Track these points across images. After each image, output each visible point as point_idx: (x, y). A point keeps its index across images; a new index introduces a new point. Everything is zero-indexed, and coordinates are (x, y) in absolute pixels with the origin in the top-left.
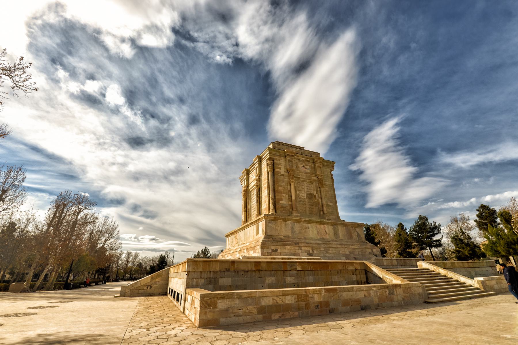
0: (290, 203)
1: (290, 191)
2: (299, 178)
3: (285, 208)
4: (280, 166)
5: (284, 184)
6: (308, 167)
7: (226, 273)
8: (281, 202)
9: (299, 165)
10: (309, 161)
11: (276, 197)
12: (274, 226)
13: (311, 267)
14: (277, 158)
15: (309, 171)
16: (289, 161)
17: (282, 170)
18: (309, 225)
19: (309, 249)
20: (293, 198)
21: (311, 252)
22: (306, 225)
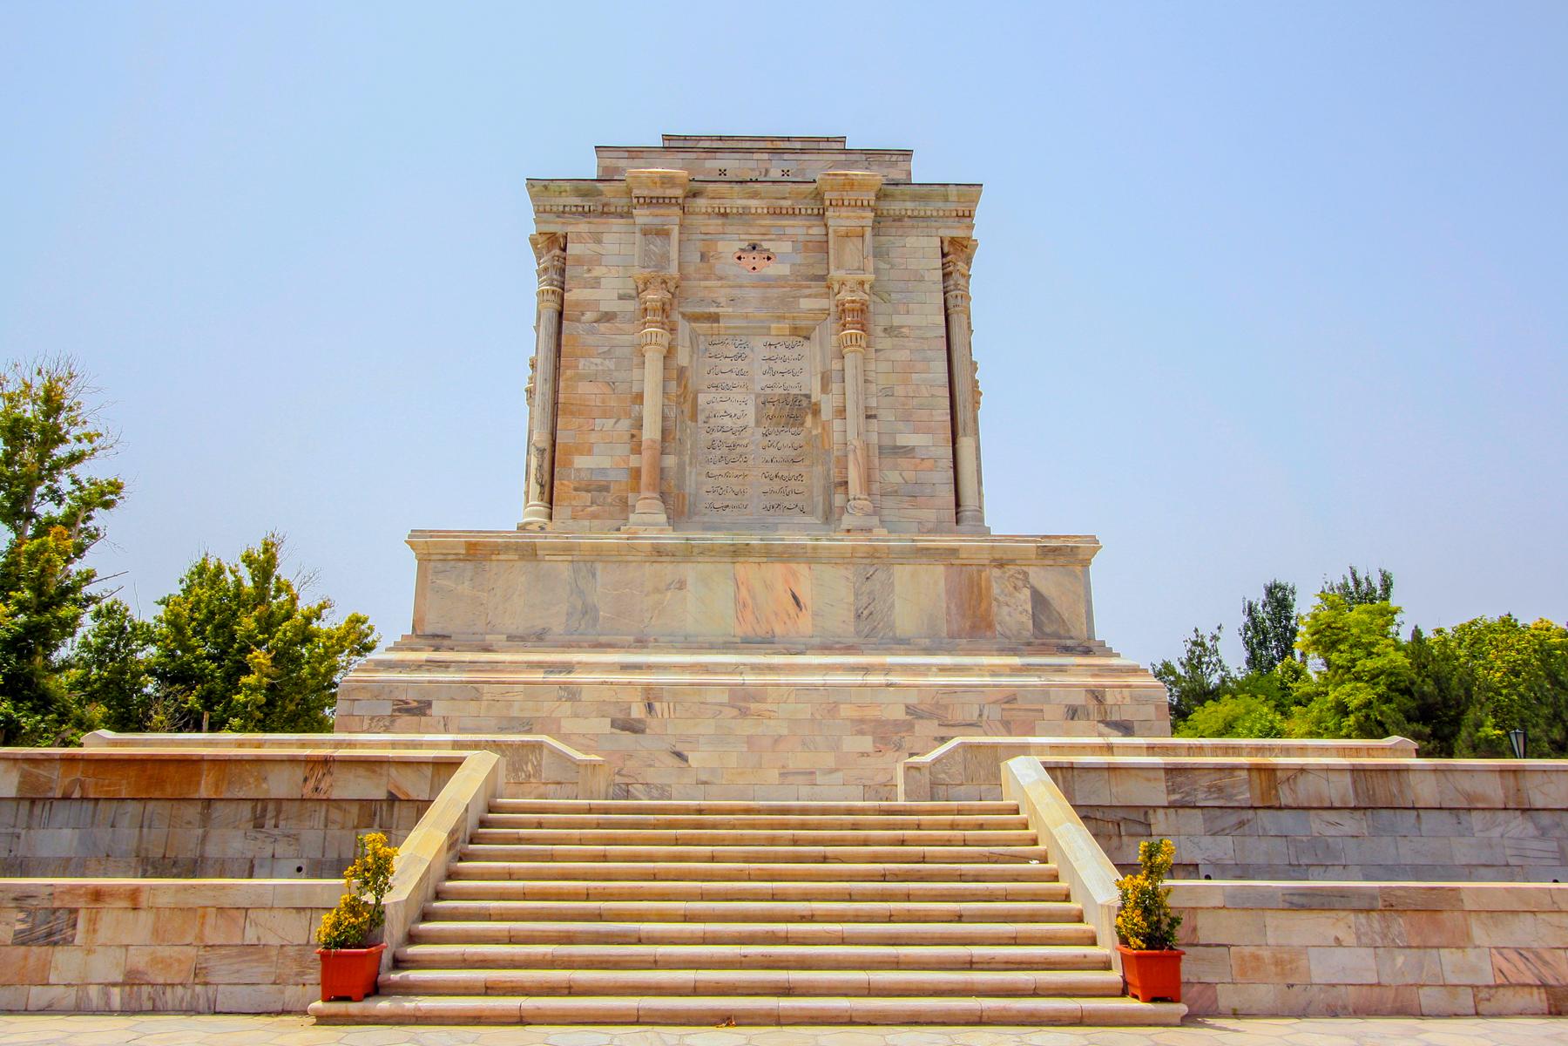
0: (634, 461)
1: (639, 398)
2: (714, 318)
3: (605, 488)
5: (610, 364)
6: (786, 247)
9: (721, 246)
12: (465, 588)
18: (689, 571)
19: (624, 697)
22: (668, 570)
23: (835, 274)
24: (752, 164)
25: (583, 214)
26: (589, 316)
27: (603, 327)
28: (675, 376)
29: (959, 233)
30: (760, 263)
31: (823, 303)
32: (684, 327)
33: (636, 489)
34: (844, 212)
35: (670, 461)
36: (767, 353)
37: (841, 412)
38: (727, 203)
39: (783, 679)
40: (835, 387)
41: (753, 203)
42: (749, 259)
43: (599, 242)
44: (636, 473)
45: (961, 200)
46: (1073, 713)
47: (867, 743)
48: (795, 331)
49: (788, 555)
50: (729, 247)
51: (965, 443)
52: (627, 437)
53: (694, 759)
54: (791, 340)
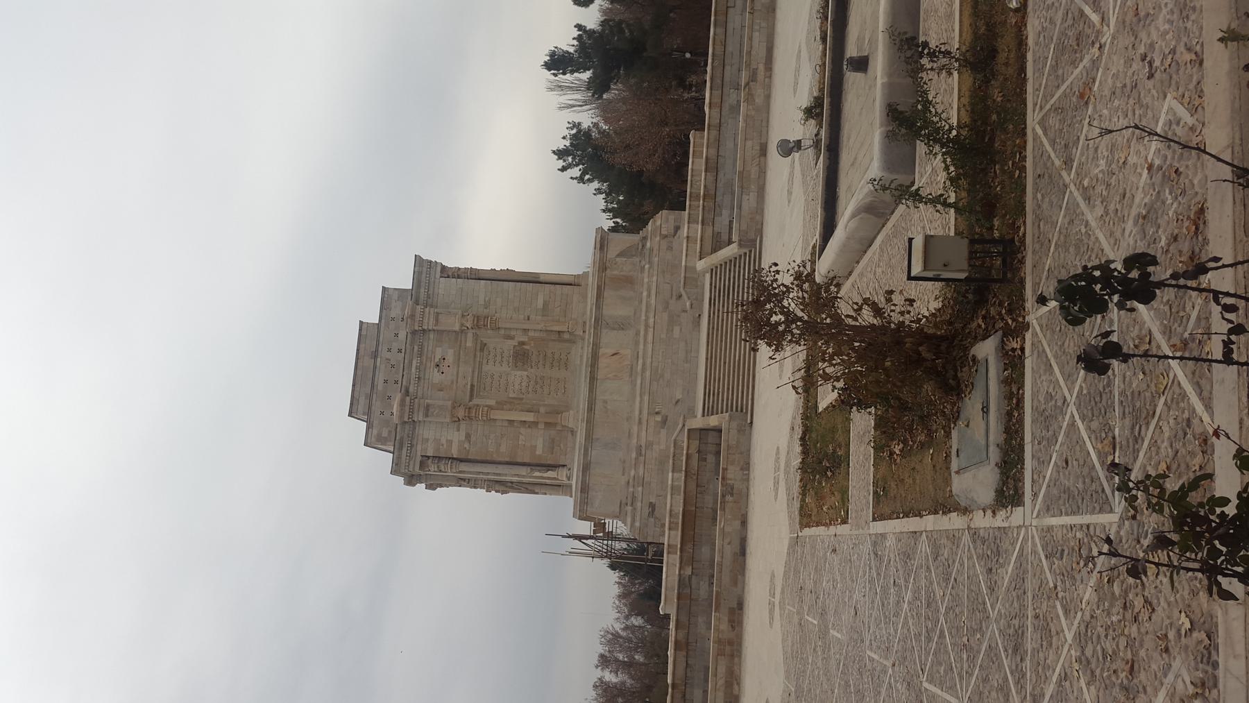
0: (541, 426)
2: (472, 386)
3: (553, 441)
4: (444, 441)
7: (687, 696)
8: (539, 452)
9: (436, 381)
10: (421, 347)
11: (527, 460)
13: (689, 547)
14: (419, 448)
15: (451, 352)
16: (427, 415)
17: (453, 439)
19: (652, 423)
20: (530, 417)
21: (659, 418)
23: (457, 328)
24: (383, 367)
25: (412, 446)
26: (466, 445)
27: (473, 439)
28: (500, 405)
29: (439, 269)
30: (446, 363)
31: (470, 335)
32: (476, 401)
33: (555, 424)
34: (426, 321)
35: (542, 410)
36: (491, 362)
37: (525, 331)
38: (413, 376)
39: (649, 360)
40: (513, 333)
41: (414, 362)
42: (445, 369)
43: (427, 440)
44: (546, 424)
45: (423, 267)
46: (670, 248)
47: (677, 330)
48: (482, 350)
49: (595, 357)
50: (436, 377)
51: (542, 279)
52: (529, 430)
53: (679, 396)
54: (486, 352)
